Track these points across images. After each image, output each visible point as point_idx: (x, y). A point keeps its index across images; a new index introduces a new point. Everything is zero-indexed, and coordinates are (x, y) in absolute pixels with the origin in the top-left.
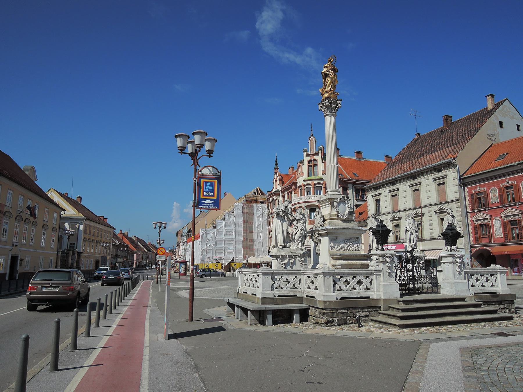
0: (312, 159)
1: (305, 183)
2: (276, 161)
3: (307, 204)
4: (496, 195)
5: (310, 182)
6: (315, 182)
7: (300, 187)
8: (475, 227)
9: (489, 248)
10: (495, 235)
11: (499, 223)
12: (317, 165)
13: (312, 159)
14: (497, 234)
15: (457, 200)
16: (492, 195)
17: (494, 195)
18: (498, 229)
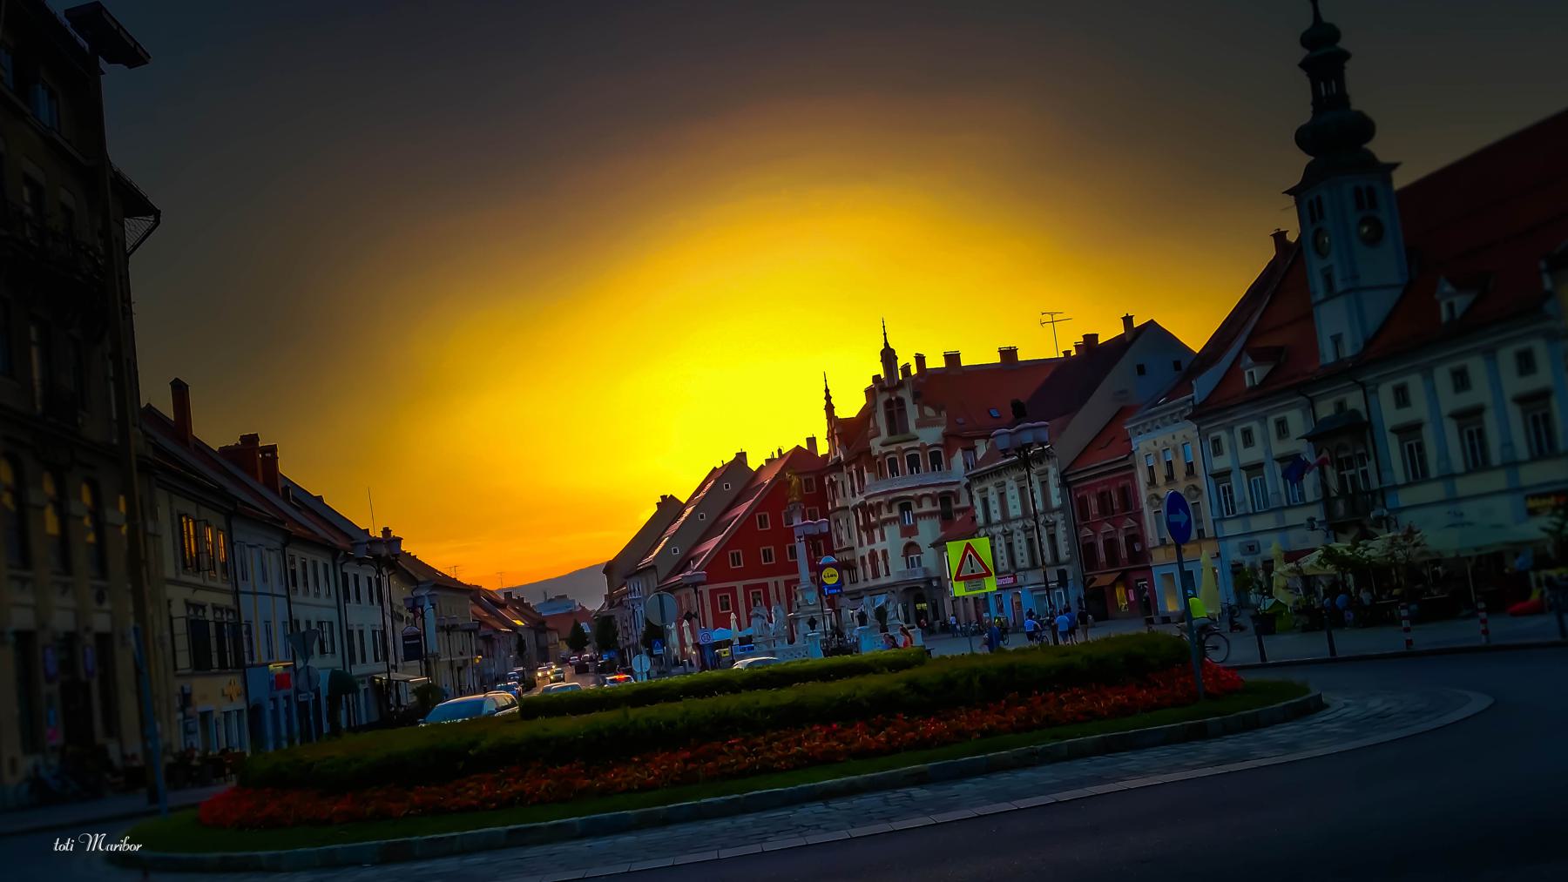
0: (893, 398)
1: (884, 450)
2: (827, 391)
3: (891, 497)
5: (893, 448)
6: (904, 446)
7: (876, 457)
8: (1083, 546)
12: (904, 410)
13: (893, 398)
15: (1061, 509)
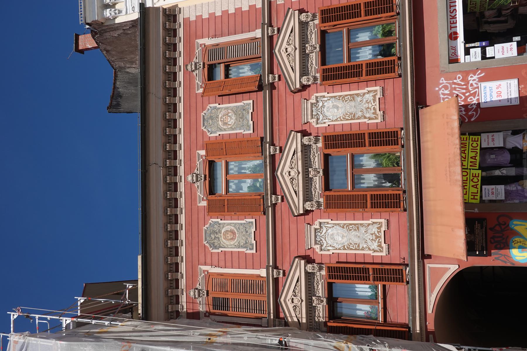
4: (228, 228)
9: (432, 291)
10: (375, 251)
11: (330, 231)
14: (375, 245)
16: (227, 243)
17: (230, 236)
18: (354, 237)
